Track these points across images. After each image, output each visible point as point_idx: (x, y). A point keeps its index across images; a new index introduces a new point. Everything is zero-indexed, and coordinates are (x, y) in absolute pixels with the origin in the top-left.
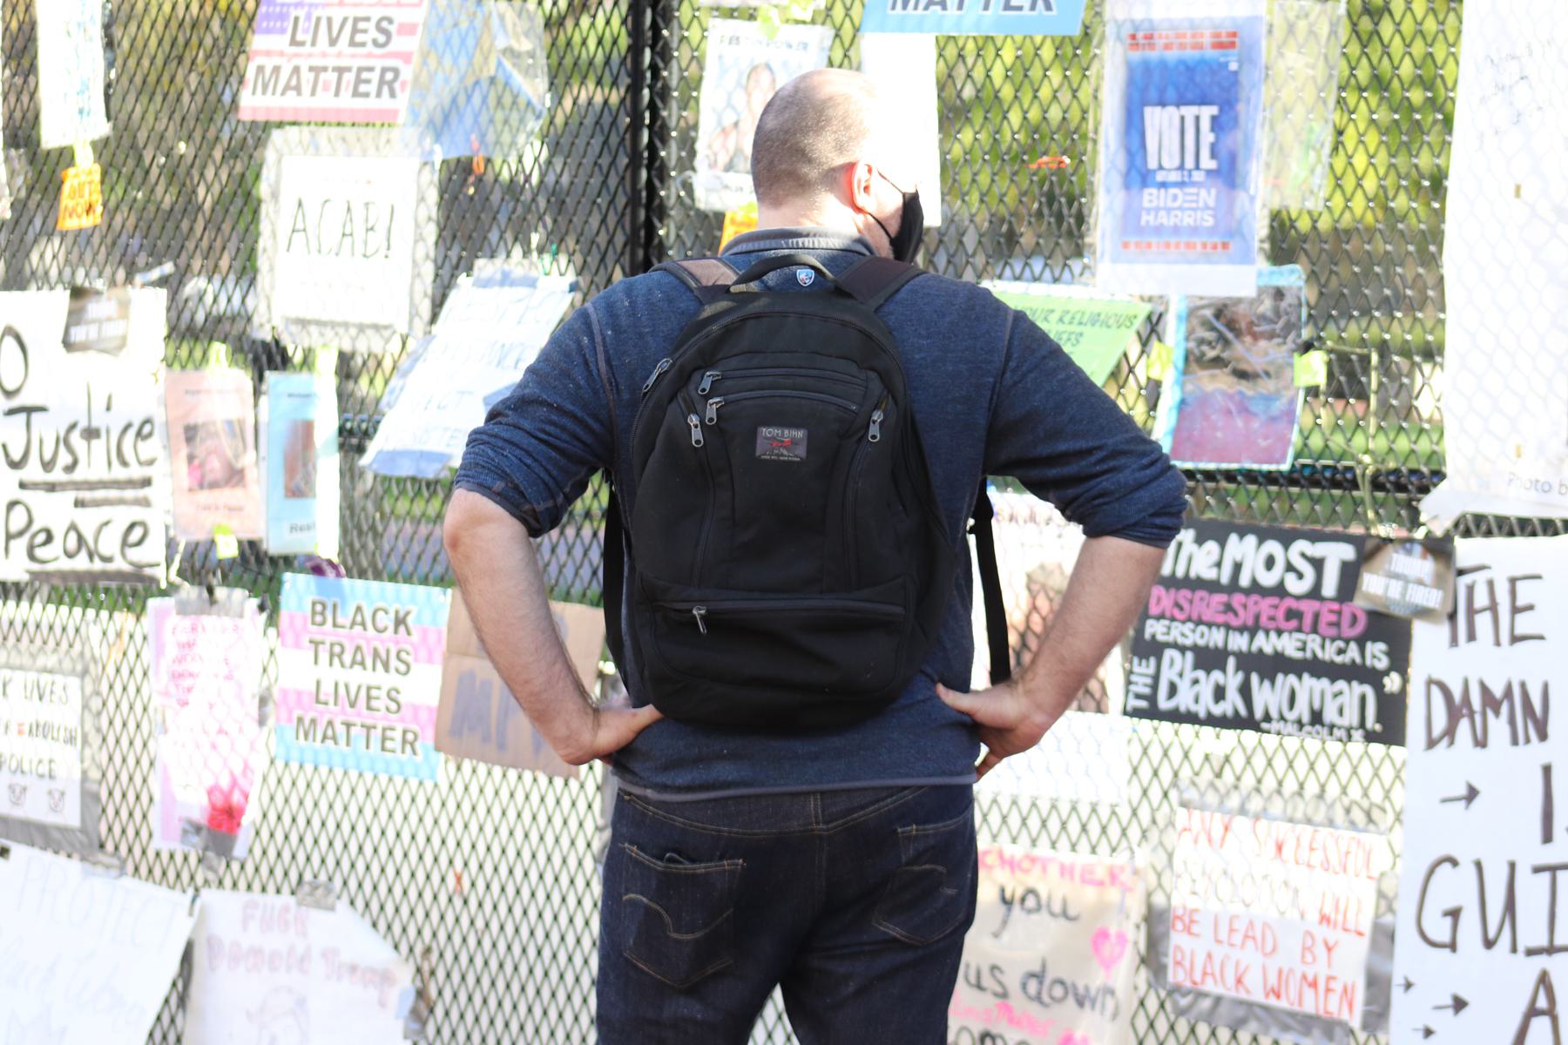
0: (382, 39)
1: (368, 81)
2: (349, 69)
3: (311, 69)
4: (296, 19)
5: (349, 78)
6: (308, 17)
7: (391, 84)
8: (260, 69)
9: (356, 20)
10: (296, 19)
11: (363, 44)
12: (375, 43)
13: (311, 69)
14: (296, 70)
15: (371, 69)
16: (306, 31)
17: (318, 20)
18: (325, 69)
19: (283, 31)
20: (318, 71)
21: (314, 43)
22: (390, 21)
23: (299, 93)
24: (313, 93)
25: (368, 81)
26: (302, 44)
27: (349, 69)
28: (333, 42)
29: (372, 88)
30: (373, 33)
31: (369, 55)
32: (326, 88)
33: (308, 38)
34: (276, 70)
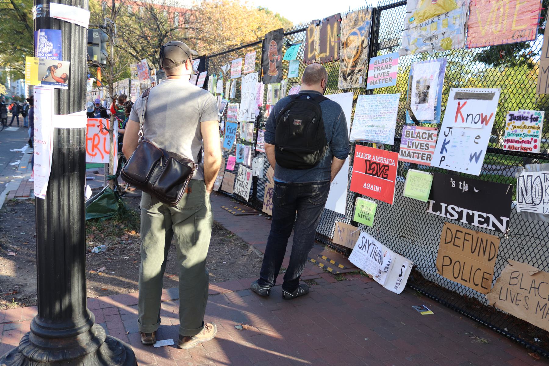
0: (427, 148)
1: (425, 157)
2: (420, 154)
3: (412, 152)
4: (409, 142)
5: (420, 155)
6: (411, 142)
7: (429, 158)
8: (402, 151)
9: (421, 144)
10: (409, 142)
11: (423, 149)
12: (425, 149)
13: (412, 152)
14: (409, 152)
15: (425, 154)
16: (411, 145)
17: (413, 143)
18: (415, 153)
19: (406, 144)
20: (414, 153)
21: (412, 147)
22: (428, 145)
23: (410, 157)
24: (413, 158)
25: (425, 157)
26: (410, 147)
27: (420, 154)
28: (416, 148)
29: (425, 158)
30: (425, 147)
31: (425, 151)
32: (416, 157)
33: (411, 146)
34: (405, 152)
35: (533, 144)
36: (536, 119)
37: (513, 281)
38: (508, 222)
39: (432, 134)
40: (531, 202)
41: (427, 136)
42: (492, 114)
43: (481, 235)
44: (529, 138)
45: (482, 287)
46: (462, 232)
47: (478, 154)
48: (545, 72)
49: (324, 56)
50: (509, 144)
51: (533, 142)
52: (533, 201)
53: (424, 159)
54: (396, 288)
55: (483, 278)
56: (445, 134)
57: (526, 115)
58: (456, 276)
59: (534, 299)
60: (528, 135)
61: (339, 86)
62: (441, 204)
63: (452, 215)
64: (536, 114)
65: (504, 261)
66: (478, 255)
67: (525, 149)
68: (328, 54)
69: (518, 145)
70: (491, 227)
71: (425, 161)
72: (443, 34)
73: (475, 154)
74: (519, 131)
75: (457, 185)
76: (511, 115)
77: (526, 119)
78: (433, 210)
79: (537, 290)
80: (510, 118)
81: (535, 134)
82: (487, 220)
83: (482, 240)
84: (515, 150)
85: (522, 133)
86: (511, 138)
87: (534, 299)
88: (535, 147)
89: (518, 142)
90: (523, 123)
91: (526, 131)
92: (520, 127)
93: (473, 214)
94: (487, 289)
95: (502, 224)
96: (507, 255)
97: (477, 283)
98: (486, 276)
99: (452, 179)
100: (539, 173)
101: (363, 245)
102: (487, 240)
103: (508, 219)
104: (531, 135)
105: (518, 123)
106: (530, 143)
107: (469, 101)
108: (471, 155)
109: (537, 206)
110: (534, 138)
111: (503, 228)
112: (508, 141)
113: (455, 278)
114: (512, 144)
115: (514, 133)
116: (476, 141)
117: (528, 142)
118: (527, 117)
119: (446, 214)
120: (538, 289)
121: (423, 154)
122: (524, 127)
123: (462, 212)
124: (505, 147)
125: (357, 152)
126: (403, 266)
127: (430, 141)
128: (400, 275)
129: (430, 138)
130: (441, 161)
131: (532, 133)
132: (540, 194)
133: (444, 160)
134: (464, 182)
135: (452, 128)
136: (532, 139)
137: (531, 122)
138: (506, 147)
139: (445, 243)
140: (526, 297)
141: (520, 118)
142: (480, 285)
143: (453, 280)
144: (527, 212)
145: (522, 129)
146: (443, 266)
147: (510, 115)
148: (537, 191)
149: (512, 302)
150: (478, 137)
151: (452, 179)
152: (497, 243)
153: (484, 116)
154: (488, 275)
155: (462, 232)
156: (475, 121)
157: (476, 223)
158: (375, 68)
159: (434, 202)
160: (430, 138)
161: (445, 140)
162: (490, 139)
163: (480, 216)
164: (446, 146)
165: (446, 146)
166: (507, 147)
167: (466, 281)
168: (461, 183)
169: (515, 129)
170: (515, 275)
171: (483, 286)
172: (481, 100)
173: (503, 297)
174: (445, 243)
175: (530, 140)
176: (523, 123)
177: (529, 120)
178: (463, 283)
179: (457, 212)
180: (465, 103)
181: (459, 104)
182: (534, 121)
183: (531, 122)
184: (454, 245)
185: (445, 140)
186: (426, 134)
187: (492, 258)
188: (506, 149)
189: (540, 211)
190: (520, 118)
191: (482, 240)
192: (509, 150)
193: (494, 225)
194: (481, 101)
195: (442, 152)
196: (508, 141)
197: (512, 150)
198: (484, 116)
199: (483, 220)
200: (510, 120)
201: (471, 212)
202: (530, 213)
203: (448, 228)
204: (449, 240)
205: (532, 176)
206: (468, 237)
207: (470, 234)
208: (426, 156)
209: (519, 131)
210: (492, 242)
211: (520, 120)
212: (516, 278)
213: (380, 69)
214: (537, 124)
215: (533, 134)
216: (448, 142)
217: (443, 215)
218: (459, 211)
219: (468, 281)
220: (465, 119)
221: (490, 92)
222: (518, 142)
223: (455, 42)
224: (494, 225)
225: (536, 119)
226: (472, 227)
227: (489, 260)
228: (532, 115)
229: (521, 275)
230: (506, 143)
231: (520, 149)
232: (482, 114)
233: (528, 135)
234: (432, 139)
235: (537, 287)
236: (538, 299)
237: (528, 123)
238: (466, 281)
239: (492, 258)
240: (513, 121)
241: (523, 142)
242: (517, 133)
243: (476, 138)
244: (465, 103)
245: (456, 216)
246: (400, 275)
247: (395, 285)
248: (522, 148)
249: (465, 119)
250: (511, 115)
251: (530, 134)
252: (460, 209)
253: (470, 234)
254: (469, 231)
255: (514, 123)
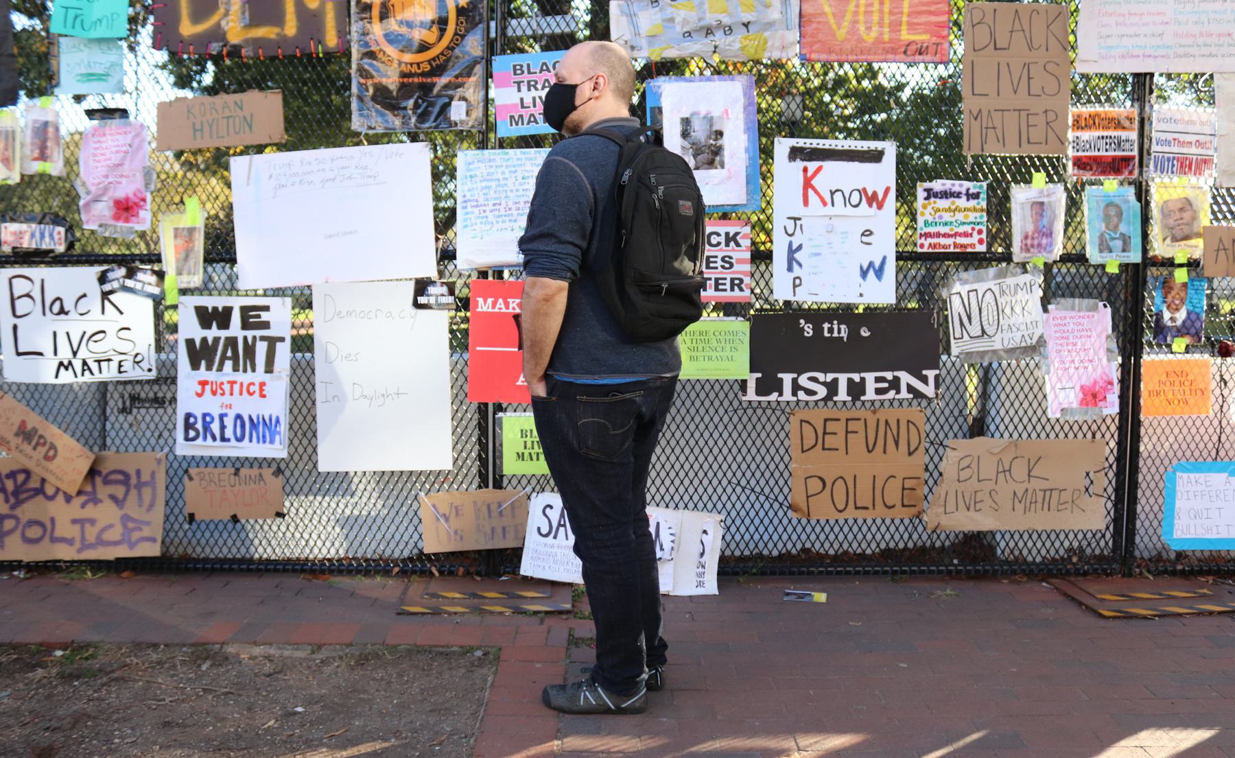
0: (727, 266)
11: (716, 268)
12: (723, 267)
15: (725, 279)
22: (731, 258)
27: (710, 279)
29: (728, 287)
30: (720, 263)
31: (721, 273)
35: (976, 237)
36: (976, 196)
37: (964, 475)
38: (937, 377)
39: (737, 234)
40: (980, 333)
41: (722, 239)
42: (887, 190)
43: (882, 415)
44: (968, 228)
45: (903, 506)
46: (838, 420)
47: (877, 265)
48: (976, 119)
49: (273, 36)
50: (930, 240)
51: (975, 233)
52: (983, 332)
53: (725, 290)
54: (700, 584)
55: (903, 489)
56: (786, 233)
57: (956, 189)
58: (841, 507)
59: (1005, 490)
60: (964, 223)
61: (357, 123)
62: (780, 375)
63: (811, 393)
64: (975, 187)
65: (936, 446)
66: (885, 452)
67: (962, 246)
68: (291, 28)
69: (943, 241)
70: (904, 394)
71: (729, 293)
72: (744, 24)
73: (871, 264)
74: (947, 217)
75: (818, 330)
76: (928, 191)
77: (958, 195)
78: (758, 393)
79: (1007, 473)
80: (925, 194)
81: (978, 220)
82: (895, 384)
83: (887, 422)
84: (943, 250)
85: (953, 220)
86: (932, 230)
87: (1005, 490)
88: (981, 242)
89: (946, 235)
90: (953, 203)
91: (960, 216)
92: (949, 210)
93: (863, 380)
94: (915, 506)
95: (908, 385)
96: (941, 435)
97: (889, 504)
98: (908, 484)
99: (802, 321)
100: (991, 284)
101: (555, 525)
102: (898, 421)
103: (937, 372)
104: (971, 223)
105: (943, 203)
106: (971, 235)
107: (829, 165)
108: (861, 268)
109: (993, 339)
110: (977, 228)
111: (929, 391)
112: (927, 235)
113: (840, 511)
114: (935, 240)
115: (937, 220)
116: (865, 239)
117: (966, 235)
118: (960, 193)
119: (794, 394)
120: (1010, 471)
121: (717, 280)
122: (956, 209)
123: (836, 381)
124: (922, 246)
125: (480, 300)
126: (705, 532)
127: (733, 250)
128: (702, 554)
129: (732, 244)
130: (795, 286)
131: (971, 219)
132: (996, 317)
133: (800, 285)
134: (835, 322)
135: (800, 219)
136: (973, 229)
137: (968, 200)
138: (925, 246)
139: (803, 451)
140: (993, 493)
141: (946, 195)
142: (899, 504)
143: (833, 515)
144: (972, 353)
145: (952, 214)
146: (808, 497)
147: (925, 190)
148: (989, 314)
149: (968, 509)
150: (868, 233)
151: (802, 321)
152: (919, 419)
153: (870, 194)
154: (914, 481)
155: (838, 420)
156: (853, 203)
157: (870, 395)
158: (519, 84)
159: (760, 375)
160: (732, 244)
161: (790, 244)
162: (455, 259)
163: (878, 380)
164: (797, 256)
165: (797, 256)
166: (926, 245)
167: (866, 508)
168: (826, 326)
169: (938, 214)
170: (964, 463)
171: (906, 503)
172: (856, 164)
173: (951, 506)
174: (803, 451)
175: (970, 231)
176: (953, 203)
177: (964, 198)
178: (860, 515)
179: (824, 384)
180: (820, 169)
181: (805, 170)
182: (974, 198)
183: (968, 200)
184: (824, 449)
185: (790, 244)
186: (718, 234)
187: (916, 449)
188: (925, 250)
189: (998, 346)
190: (946, 195)
191: (887, 422)
192: (930, 250)
193: (910, 389)
194: (855, 165)
195: (790, 269)
196: (927, 235)
197: (936, 251)
198: (870, 194)
199: (886, 385)
200: (926, 199)
201: (856, 377)
202: (978, 352)
203: (802, 421)
204: (809, 442)
205: (976, 290)
206: (853, 426)
207: (859, 419)
208: (728, 282)
209: (947, 217)
210: (908, 421)
211: (947, 198)
212: (968, 467)
213: (539, 86)
214: (978, 204)
215: (974, 220)
216: (800, 247)
217: (787, 395)
218: (829, 380)
219: (871, 507)
220: (828, 200)
221: (873, 148)
222: (946, 235)
223: (773, 44)
224: (910, 389)
225: (976, 196)
226: (840, 405)
227: (910, 454)
228: (968, 190)
229: (976, 459)
230: (923, 239)
231: (952, 247)
232: (864, 190)
233: (964, 223)
234: (738, 245)
235: (1007, 468)
236: (1014, 486)
237: (962, 202)
238: (866, 508)
239: (916, 449)
240: (932, 200)
241: (956, 234)
242: (943, 220)
243: (863, 235)
244: (820, 169)
245: (822, 392)
246: (702, 554)
247: (695, 580)
248: (955, 245)
249: (828, 200)
250: (928, 191)
251: (968, 221)
252: (830, 377)
253: (859, 419)
254: (854, 413)
255: (935, 203)
